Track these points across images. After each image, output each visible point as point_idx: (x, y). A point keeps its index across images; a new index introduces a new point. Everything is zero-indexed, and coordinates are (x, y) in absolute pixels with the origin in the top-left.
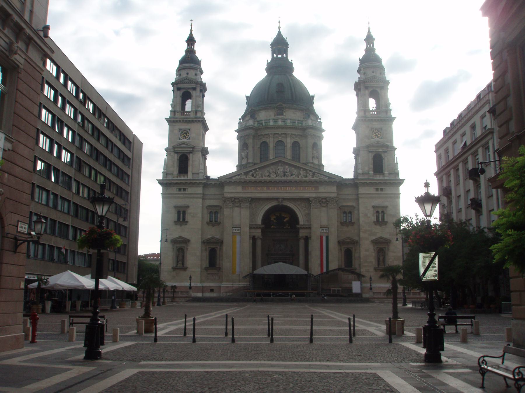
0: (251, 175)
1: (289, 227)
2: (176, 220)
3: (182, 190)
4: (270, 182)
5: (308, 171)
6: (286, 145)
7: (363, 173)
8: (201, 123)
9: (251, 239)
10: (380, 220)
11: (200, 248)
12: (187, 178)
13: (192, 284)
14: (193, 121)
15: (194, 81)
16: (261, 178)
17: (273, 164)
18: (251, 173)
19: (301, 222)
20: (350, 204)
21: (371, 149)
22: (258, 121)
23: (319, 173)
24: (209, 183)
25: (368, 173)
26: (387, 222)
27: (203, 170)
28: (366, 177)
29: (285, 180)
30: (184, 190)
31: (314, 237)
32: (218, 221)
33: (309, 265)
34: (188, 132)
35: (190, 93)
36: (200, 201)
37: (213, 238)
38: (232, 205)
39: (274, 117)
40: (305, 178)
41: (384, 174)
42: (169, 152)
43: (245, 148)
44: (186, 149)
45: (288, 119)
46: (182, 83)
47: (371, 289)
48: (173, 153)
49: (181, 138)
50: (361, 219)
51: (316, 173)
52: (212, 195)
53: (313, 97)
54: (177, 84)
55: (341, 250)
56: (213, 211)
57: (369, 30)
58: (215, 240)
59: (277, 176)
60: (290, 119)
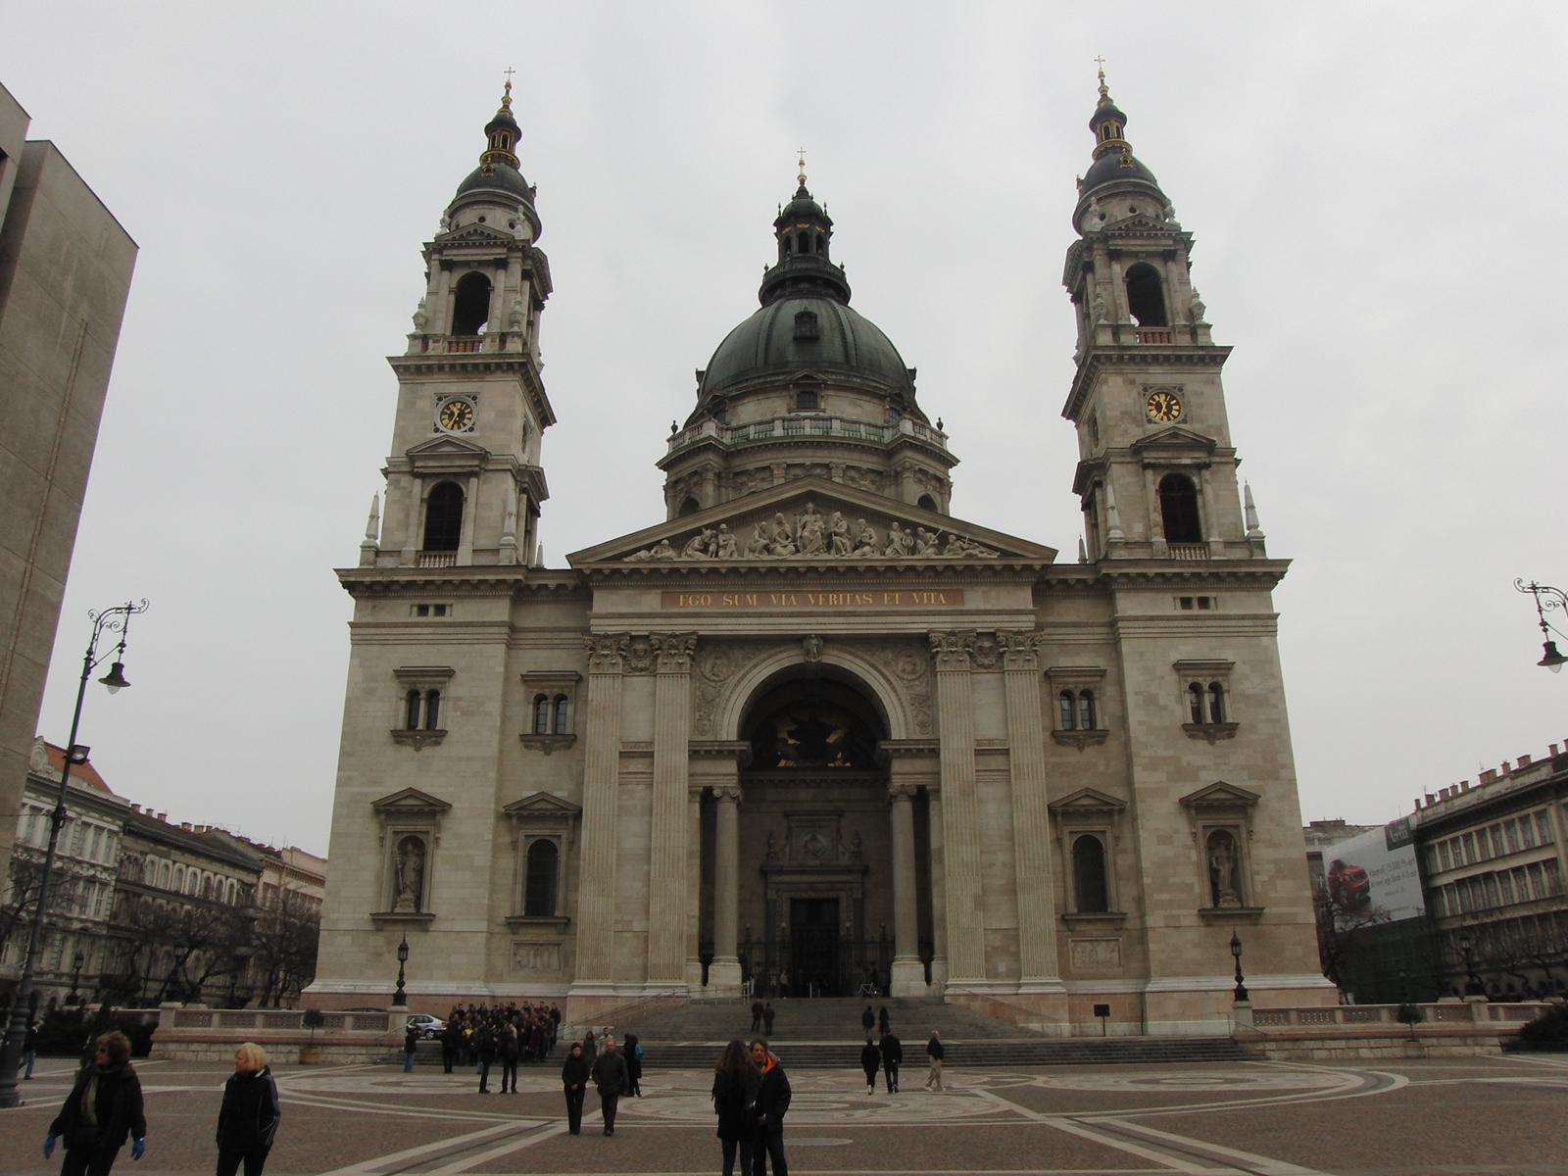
1: (848, 764)
2: (401, 724)
3: (431, 610)
4: (773, 571)
7: (1127, 543)
9: (698, 799)
10: (1209, 719)
11: (490, 837)
14: (487, 367)
16: (736, 557)
17: (784, 506)
18: (697, 541)
20: (1083, 661)
21: (1150, 457)
23: (963, 535)
24: (535, 583)
25: (1147, 544)
26: (1236, 725)
27: (513, 535)
28: (1140, 554)
29: (829, 564)
30: (440, 610)
31: (949, 788)
33: (936, 901)
34: (468, 406)
35: (487, 278)
36: (501, 649)
37: (543, 797)
38: (620, 661)
39: (787, 415)
40: (909, 557)
41: (1208, 544)
42: (391, 476)
44: (457, 463)
46: (460, 246)
47: (1241, 994)
48: (405, 480)
49: (442, 428)
50: (1135, 717)
51: (952, 538)
52: (542, 630)
53: (915, 371)
54: (440, 252)
56: (547, 692)
57: (1104, 96)
58: (550, 806)
59: (798, 551)
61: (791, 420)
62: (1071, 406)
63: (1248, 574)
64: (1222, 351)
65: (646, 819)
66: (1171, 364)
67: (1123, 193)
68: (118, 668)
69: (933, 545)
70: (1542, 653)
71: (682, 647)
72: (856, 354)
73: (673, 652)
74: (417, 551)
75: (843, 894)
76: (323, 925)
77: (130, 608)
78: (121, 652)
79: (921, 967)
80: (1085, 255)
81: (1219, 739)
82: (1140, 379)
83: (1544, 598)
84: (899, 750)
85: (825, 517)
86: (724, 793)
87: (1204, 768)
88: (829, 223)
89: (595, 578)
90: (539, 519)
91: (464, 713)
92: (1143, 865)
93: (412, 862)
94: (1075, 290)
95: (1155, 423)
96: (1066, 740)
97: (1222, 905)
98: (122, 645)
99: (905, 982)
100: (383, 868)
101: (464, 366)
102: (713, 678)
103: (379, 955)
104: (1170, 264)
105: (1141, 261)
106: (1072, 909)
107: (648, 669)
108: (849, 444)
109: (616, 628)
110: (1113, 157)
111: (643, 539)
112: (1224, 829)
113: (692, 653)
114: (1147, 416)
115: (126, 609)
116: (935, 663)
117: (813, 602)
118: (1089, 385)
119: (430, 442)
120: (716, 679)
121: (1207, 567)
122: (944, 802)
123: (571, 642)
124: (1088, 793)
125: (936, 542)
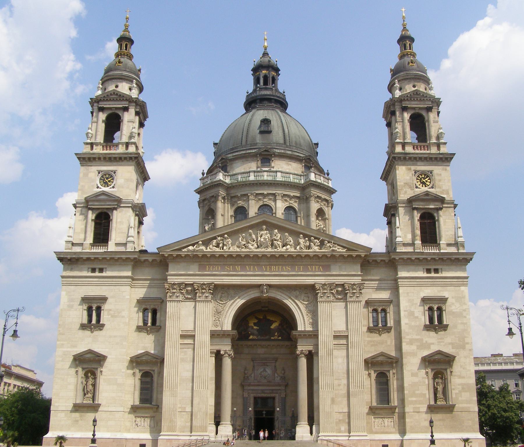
0: (214, 244)
1: (280, 338)
2: (85, 321)
3: (97, 270)
4: (247, 256)
5: (313, 238)
6: (274, 211)
7: (403, 244)
8: (134, 162)
9: (214, 355)
10: (436, 323)
12: (106, 250)
13: (98, 435)
14: (120, 158)
15: (125, 96)
17: (251, 227)
19: (300, 328)
22: (230, 176)
24: (143, 259)
25: (413, 244)
26: (447, 326)
27: (133, 237)
28: (410, 249)
31: (322, 352)
32: (158, 324)
34: (112, 176)
37: (147, 354)
41: (439, 244)
42: (77, 209)
43: (210, 217)
45: (279, 172)
46: (107, 100)
48: (84, 210)
50: (404, 321)
53: (317, 144)
54: (98, 102)
55: (369, 374)
56: (148, 307)
57: (405, 29)
59: (258, 247)
60: (281, 172)
61: (258, 172)
62: (384, 176)
63: (455, 258)
64: (450, 155)
65: (192, 363)
66: (427, 161)
67: (410, 78)
68: (15, 331)
69: (318, 246)
70: (508, 331)
71: (207, 288)
72: (289, 139)
73: (204, 291)
74: (90, 243)
75: (277, 395)
76: (52, 408)
77: (18, 310)
78: (16, 326)
79: (308, 428)
80: (392, 107)
81: (440, 331)
82: (413, 168)
83: (510, 312)
84: (301, 335)
85: (270, 231)
86: (225, 353)
87: (433, 344)
88: (277, 70)
89: (169, 258)
90: (143, 225)
91: (112, 316)
92: (405, 386)
93: (91, 381)
94: (388, 121)
95: (419, 188)
96: (373, 330)
97: (439, 403)
98: (16, 323)
99: (302, 434)
100: (77, 384)
101: (110, 159)
102: (221, 302)
103: (77, 421)
104: (430, 113)
105: (417, 111)
106: (374, 404)
107: (193, 298)
108: (285, 184)
109: (178, 280)
110: (407, 59)
111: (192, 241)
112: (441, 370)
113: (212, 291)
114: (416, 185)
115: (17, 310)
116: (317, 297)
117: (264, 269)
118: (391, 169)
119: (97, 193)
120: (222, 303)
121: (438, 255)
122: (320, 358)
123: (159, 285)
124: (382, 354)
125: (319, 244)
